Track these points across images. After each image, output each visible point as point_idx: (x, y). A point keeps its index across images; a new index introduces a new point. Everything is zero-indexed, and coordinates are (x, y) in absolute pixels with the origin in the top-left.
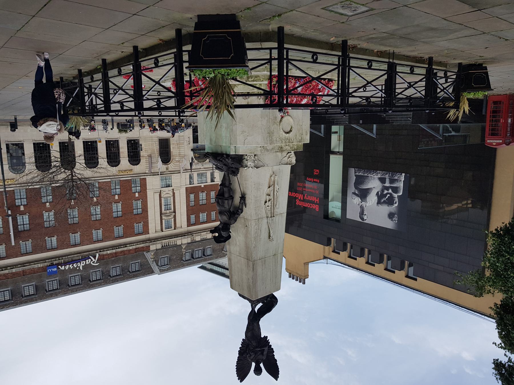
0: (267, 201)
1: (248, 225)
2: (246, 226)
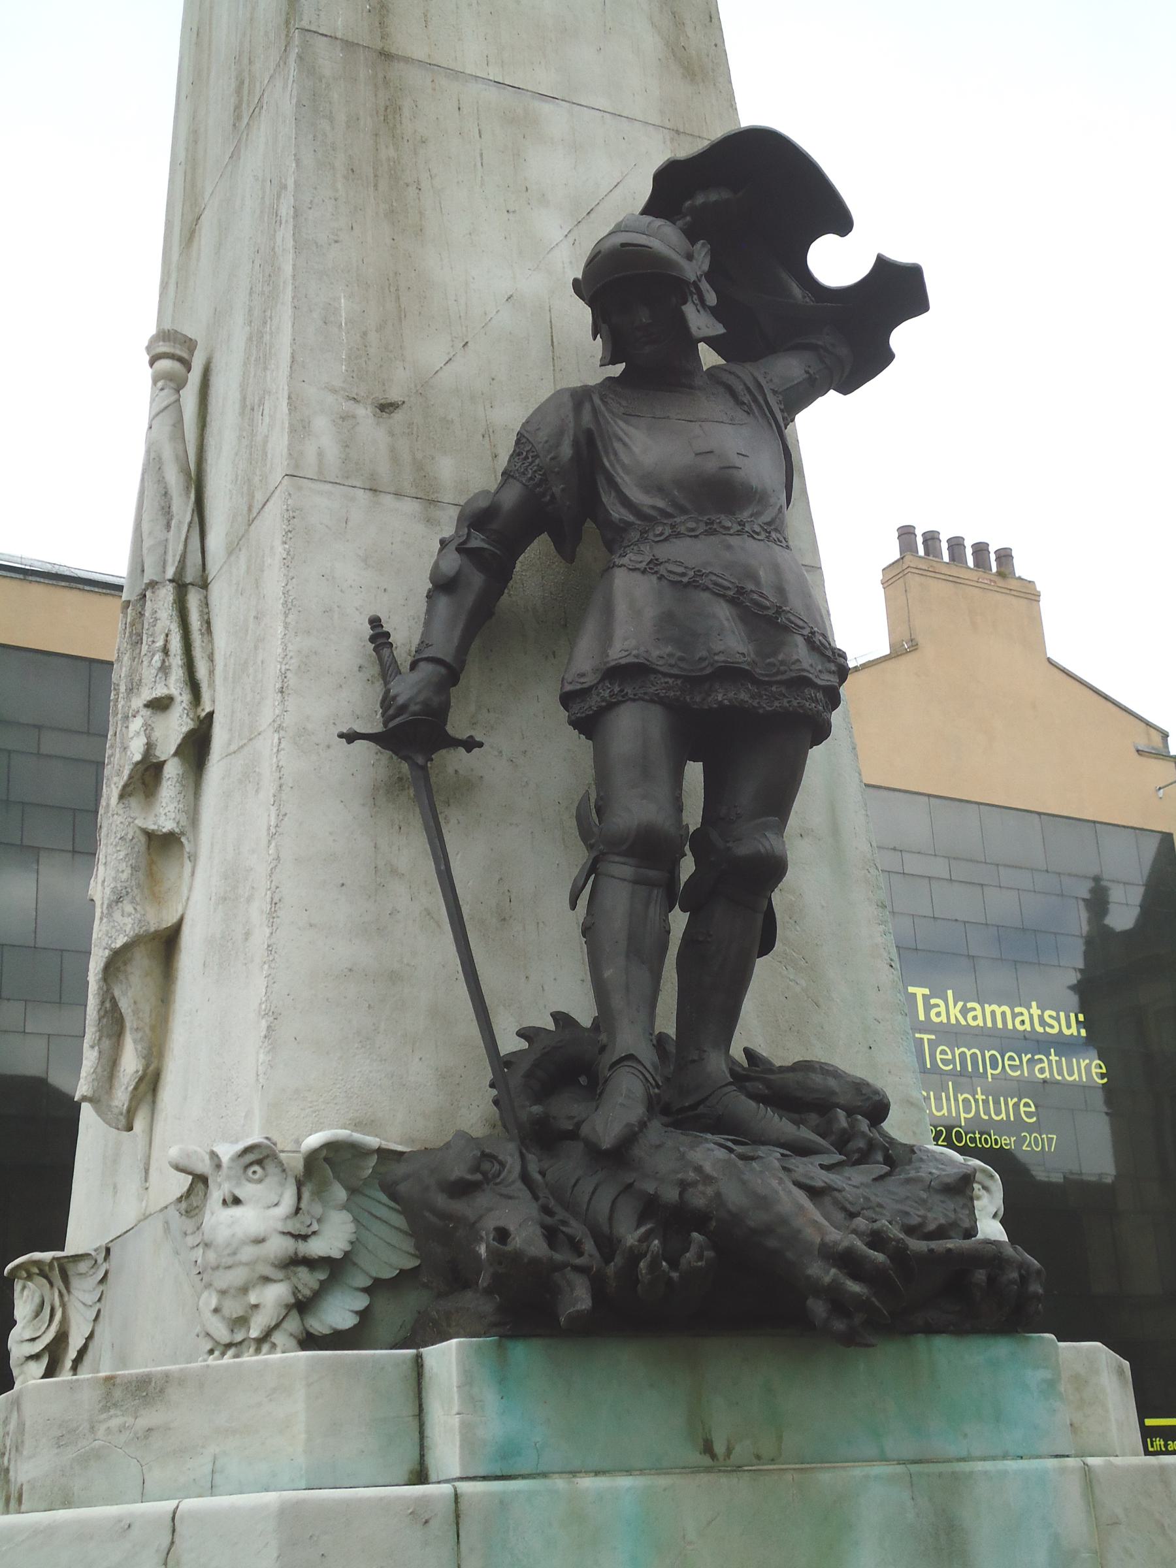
0: (173, 770)
1: (348, 419)
2: (386, 408)
